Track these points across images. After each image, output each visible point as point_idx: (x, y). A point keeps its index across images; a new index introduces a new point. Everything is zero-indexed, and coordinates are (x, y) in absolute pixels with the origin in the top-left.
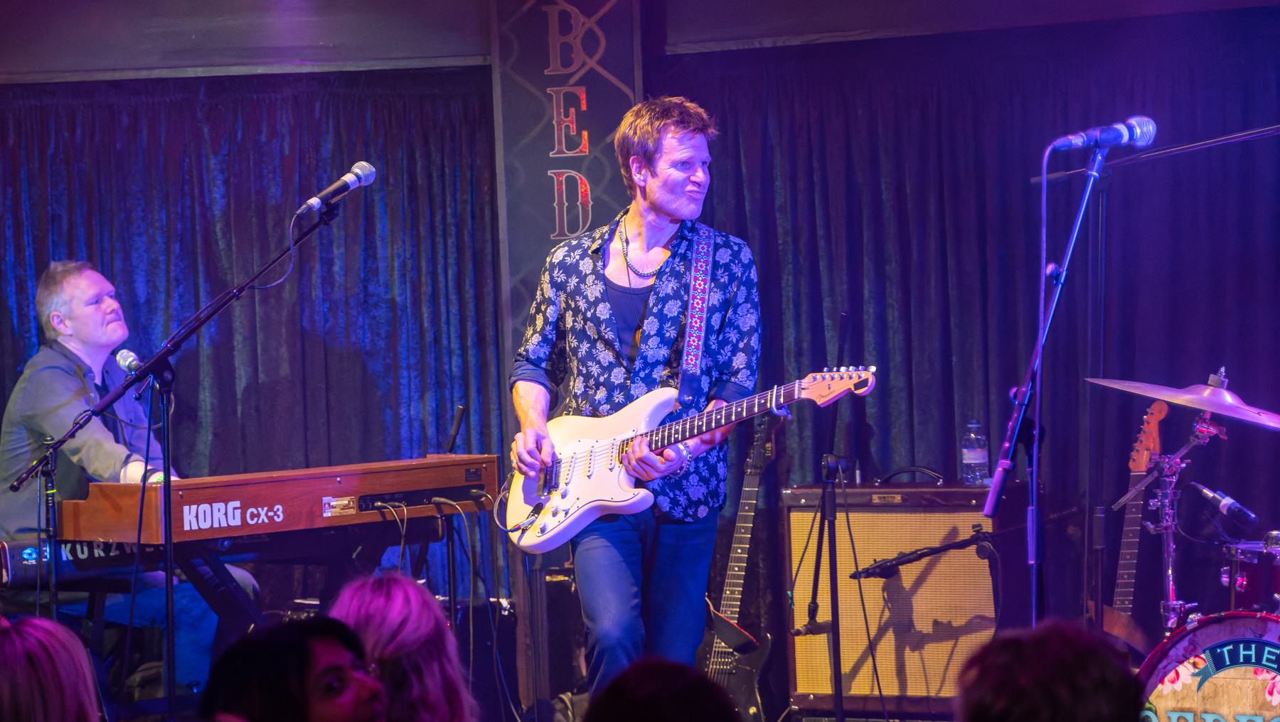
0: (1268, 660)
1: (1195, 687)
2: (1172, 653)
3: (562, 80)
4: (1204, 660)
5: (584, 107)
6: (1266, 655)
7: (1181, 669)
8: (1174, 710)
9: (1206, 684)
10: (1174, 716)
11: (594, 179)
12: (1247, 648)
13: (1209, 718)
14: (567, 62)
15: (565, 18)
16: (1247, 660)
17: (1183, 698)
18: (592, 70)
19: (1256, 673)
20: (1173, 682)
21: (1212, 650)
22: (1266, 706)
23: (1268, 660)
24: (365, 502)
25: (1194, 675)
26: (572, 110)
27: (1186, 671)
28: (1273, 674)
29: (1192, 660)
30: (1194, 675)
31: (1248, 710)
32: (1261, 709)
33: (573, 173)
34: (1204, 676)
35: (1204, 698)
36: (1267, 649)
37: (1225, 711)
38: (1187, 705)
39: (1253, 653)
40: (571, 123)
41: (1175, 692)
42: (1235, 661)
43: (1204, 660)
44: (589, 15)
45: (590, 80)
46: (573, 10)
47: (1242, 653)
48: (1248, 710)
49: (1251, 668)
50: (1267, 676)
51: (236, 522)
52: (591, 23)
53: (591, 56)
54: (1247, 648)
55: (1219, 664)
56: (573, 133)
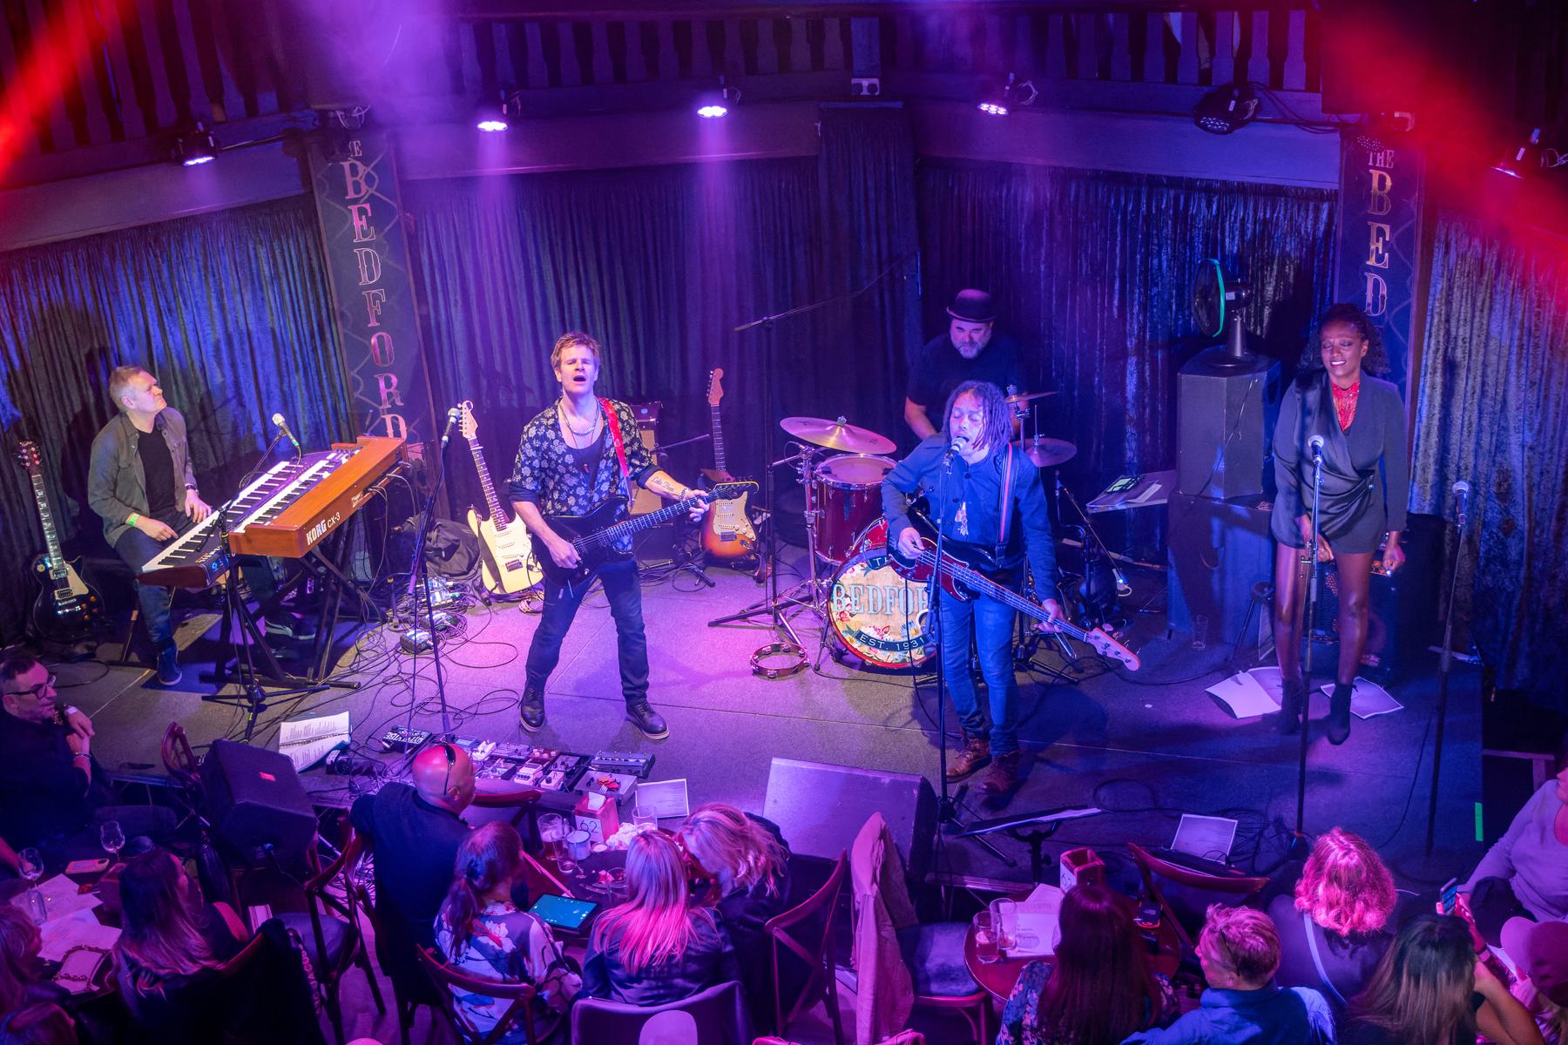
2: (851, 561)
3: (355, 201)
5: (370, 214)
10: (853, 587)
11: (381, 254)
13: (871, 588)
14: (357, 191)
15: (354, 169)
18: (372, 195)
21: (871, 560)
24: (365, 491)
26: (364, 217)
27: (858, 568)
31: (890, 584)
33: (368, 250)
34: (867, 571)
38: (859, 582)
40: (364, 222)
44: (367, 166)
45: (372, 199)
46: (358, 163)
48: (890, 584)
51: (324, 530)
52: (369, 169)
53: (371, 186)
56: (365, 228)
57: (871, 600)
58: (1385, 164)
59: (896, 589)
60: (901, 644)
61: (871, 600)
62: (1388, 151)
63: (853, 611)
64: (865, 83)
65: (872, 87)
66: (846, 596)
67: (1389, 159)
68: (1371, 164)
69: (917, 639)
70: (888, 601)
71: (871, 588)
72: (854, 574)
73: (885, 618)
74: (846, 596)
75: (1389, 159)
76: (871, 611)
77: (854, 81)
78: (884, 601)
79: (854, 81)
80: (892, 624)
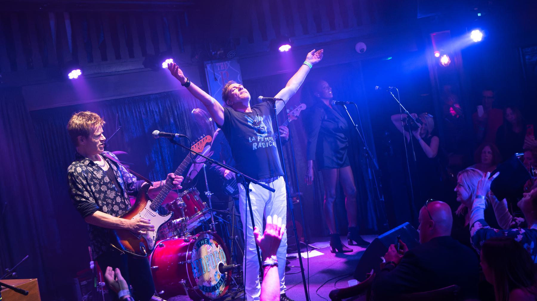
1: (196, 254)
6: (205, 241)
16: (203, 244)
19: (205, 246)
22: (208, 252)
32: (208, 253)
36: (205, 240)
39: (203, 242)
49: (204, 245)
54: (202, 241)
58: (224, 68)
59: (208, 256)
60: (216, 285)
62: (225, 63)
66: (195, 268)
67: (225, 66)
68: (219, 69)
69: (220, 280)
75: (225, 66)
78: (206, 265)
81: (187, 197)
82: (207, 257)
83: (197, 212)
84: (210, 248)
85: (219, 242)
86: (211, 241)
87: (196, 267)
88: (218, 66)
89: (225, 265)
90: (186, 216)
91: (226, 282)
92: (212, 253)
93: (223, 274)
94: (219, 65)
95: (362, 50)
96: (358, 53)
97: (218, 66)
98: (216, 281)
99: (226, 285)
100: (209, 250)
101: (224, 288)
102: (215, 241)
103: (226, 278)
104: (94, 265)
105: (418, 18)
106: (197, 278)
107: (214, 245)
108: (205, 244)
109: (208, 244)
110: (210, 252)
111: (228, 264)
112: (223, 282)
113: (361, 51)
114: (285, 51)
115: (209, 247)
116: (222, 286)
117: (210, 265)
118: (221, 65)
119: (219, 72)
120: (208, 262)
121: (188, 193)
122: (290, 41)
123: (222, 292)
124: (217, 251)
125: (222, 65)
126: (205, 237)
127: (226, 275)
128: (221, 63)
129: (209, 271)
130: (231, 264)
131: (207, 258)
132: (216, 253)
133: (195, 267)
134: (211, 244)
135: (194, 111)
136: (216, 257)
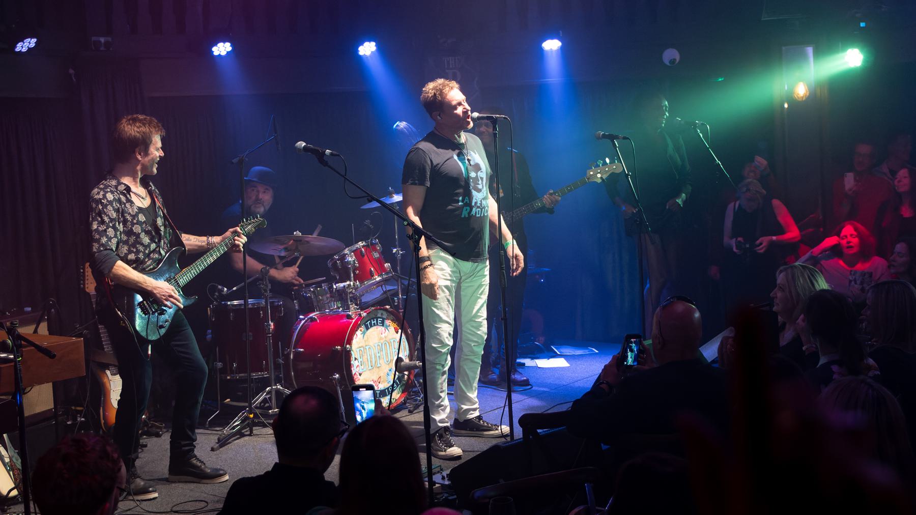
0: (380, 323)
4: (363, 328)
6: (379, 322)
7: (357, 333)
8: (358, 348)
9: (365, 336)
10: (358, 350)
12: (374, 321)
17: (360, 343)
20: (356, 338)
22: (381, 339)
23: (380, 323)
25: (361, 334)
27: (359, 333)
28: (381, 327)
29: (360, 329)
30: (361, 334)
34: (364, 333)
35: (365, 341)
36: (379, 319)
37: (371, 344)
38: (360, 345)
39: (375, 322)
41: (357, 342)
42: (371, 326)
43: (363, 328)
47: (373, 322)
49: (375, 327)
50: (381, 329)
54: (374, 321)
55: (367, 328)
57: (369, 358)
60: (388, 388)
61: (369, 358)
63: (361, 371)
64: (102, 40)
65: (106, 43)
70: (378, 355)
71: (367, 348)
72: (358, 339)
73: (377, 370)
74: (356, 359)
76: (370, 368)
77: (94, 38)
78: (375, 356)
79: (94, 38)
80: (382, 375)
81: (361, 251)
82: (379, 345)
83: (373, 276)
84: (384, 333)
85: (402, 325)
86: (388, 322)
87: (359, 358)
88: (446, 61)
89: (406, 360)
90: (355, 280)
91: (403, 387)
92: (387, 340)
93: (401, 375)
94: (447, 60)
95: (673, 61)
96: (668, 66)
97: (446, 61)
98: (388, 383)
99: (403, 392)
100: (383, 336)
101: (399, 395)
102: (395, 323)
103: (405, 381)
104: (211, 336)
105: (762, 19)
106: (358, 374)
107: (392, 329)
108: (377, 325)
109: (383, 326)
110: (385, 339)
111: (411, 360)
112: (400, 386)
113: (670, 62)
114: (551, 49)
115: (384, 331)
116: (396, 391)
117: (382, 357)
118: (451, 59)
119: (447, 71)
120: (378, 353)
121: (363, 246)
122: (561, 35)
123: (396, 400)
124: (396, 339)
125: (452, 60)
126: (379, 315)
127: (406, 377)
128: (450, 58)
129: (378, 367)
130: (414, 360)
131: (379, 348)
132: (394, 341)
133: (357, 358)
134: (387, 327)
135: (397, 126)
136: (393, 349)
